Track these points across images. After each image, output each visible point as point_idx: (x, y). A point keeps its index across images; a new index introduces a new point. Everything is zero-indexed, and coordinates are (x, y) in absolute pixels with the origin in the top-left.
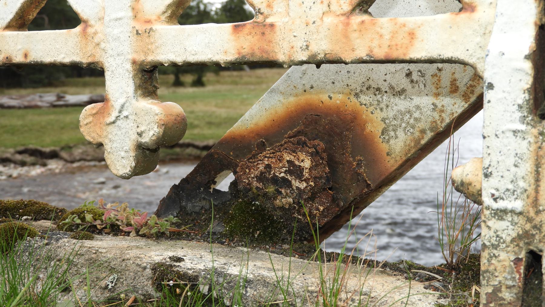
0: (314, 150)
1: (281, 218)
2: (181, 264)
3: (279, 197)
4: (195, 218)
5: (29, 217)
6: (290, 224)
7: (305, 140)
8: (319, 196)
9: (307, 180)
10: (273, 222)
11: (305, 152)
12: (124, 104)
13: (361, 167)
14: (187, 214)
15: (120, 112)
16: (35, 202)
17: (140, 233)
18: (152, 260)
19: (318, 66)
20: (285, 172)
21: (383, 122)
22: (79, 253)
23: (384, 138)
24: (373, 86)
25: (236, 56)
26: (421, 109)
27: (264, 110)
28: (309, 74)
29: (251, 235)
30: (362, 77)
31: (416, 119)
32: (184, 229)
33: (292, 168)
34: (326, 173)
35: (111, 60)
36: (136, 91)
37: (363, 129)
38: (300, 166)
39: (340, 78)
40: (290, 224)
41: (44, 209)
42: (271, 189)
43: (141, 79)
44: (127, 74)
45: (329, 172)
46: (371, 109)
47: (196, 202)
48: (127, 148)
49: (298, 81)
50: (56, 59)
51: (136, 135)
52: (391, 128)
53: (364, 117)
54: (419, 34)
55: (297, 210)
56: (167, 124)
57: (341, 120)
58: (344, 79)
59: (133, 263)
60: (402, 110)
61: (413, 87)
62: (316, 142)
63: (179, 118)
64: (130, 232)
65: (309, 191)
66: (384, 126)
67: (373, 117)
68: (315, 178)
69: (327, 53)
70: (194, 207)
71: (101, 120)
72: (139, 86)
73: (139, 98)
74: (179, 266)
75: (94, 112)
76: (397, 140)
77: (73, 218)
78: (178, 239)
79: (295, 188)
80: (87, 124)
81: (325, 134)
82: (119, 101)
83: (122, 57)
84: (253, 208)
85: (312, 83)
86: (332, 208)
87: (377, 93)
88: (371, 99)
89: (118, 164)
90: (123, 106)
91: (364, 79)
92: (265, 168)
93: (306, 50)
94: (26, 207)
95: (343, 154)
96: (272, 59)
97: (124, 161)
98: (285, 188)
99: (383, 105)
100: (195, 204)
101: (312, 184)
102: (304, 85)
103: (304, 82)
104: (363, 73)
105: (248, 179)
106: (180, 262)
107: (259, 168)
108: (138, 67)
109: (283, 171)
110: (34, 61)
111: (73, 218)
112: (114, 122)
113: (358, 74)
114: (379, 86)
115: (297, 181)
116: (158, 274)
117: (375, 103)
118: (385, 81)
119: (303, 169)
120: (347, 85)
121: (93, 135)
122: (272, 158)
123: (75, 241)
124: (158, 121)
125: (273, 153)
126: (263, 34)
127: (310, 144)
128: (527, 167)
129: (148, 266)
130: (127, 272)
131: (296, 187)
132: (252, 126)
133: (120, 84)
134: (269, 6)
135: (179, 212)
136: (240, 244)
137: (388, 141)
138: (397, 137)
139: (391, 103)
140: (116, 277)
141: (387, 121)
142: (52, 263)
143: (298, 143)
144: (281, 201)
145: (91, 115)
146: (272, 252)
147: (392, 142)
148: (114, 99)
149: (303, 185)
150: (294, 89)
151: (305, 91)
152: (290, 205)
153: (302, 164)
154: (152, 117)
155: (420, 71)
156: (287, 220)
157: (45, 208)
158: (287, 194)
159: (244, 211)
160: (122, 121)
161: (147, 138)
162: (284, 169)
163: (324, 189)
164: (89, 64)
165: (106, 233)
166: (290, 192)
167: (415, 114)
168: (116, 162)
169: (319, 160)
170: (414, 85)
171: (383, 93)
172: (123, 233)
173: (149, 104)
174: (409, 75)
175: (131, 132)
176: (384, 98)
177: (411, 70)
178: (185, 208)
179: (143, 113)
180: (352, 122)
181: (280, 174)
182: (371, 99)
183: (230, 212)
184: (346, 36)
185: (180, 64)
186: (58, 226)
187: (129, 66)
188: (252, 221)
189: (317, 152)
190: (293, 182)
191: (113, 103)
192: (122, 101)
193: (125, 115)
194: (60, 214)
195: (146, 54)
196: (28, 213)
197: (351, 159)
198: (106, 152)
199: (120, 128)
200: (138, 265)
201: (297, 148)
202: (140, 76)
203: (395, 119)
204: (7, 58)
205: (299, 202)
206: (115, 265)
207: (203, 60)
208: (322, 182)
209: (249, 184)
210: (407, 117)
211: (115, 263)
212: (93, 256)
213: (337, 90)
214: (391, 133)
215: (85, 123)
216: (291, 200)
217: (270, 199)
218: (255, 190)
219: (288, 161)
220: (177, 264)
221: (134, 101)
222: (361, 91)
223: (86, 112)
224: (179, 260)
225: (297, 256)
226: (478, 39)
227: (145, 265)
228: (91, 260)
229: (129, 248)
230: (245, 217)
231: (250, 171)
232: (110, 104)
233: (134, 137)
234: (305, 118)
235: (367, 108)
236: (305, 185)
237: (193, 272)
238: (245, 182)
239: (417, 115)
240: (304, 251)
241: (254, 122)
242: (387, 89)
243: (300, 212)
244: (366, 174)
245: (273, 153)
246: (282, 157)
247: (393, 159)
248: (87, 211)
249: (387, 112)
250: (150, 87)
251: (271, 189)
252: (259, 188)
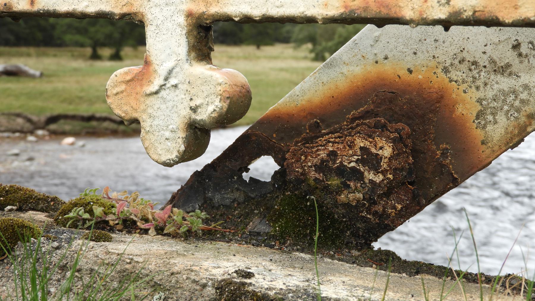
0: (396, 135)
1: (344, 217)
2: (252, 281)
3: (345, 192)
4: (224, 213)
5: (15, 208)
6: (354, 224)
7: (385, 122)
8: (396, 192)
9: (384, 172)
10: (334, 221)
11: (385, 137)
12: (173, 69)
13: (447, 157)
14: (213, 207)
15: (166, 79)
16: (18, 188)
17: (165, 232)
18: (211, 275)
19: (447, 29)
20: (357, 161)
21: (478, 104)
22: (106, 262)
23: (479, 123)
24: (468, 59)
25: (342, 10)
26: (530, 89)
27: (321, 84)
28: (383, 42)
29: (308, 238)
30: (454, 47)
31: (522, 101)
32: (214, 227)
33: (365, 156)
34: (409, 164)
35: (156, 11)
36: (189, 52)
37: (453, 111)
38: (377, 154)
39: (424, 48)
40: (354, 224)
41: (31, 197)
42: (335, 182)
43: (196, 37)
44: (179, 30)
45: (413, 163)
46: (464, 87)
47: (227, 194)
48: (174, 127)
49: (368, 50)
50: (76, 7)
51: (188, 110)
52: (489, 111)
53: (454, 96)
55: (367, 208)
56: (232, 97)
57: (424, 99)
58: (429, 49)
59: (187, 278)
60: (505, 89)
61: (521, 62)
62: (400, 125)
63: (244, 90)
64: (149, 229)
65: (385, 185)
66: (480, 108)
67: (467, 96)
68: (396, 169)
69: (477, 9)
70: (223, 198)
71: (138, 89)
72: (193, 46)
73: (193, 62)
74: (251, 283)
75: (128, 78)
76: (496, 126)
77: (79, 211)
78: (212, 240)
79: (367, 181)
80: (117, 94)
81: (403, 116)
82: (164, 64)
83: (173, 8)
84: (308, 204)
85: (387, 52)
86: (412, 207)
87: (473, 67)
88: (464, 75)
89: (160, 147)
90: (170, 72)
91: (456, 50)
92: (328, 155)
93: (447, 6)
94: (7, 195)
95: (424, 141)
96: (395, 15)
97: (169, 144)
98: (355, 180)
99: (479, 83)
100: (225, 196)
101: (391, 176)
102: (376, 54)
103: (375, 52)
104: (456, 42)
105: (302, 167)
106: (249, 278)
107: (319, 155)
108: (194, 21)
109: (353, 159)
110: (44, 10)
111: (79, 211)
112: (156, 93)
113: (449, 43)
114: (476, 59)
115: (372, 172)
116: (227, 296)
117: (469, 80)
118: (484, 53)
119: (381, 158)
120: (434, 56)
121: (125, 108)
122: (338, 143)
123: (92, 243)
124: (221, 92)
125: (339, 137)
127: (392, 128)
129: (210, 283)
130: (179, 291)
131: (370, 180)
132: (304, 102)
133: (167, 41)
135: (202, 205)
136: (295, 248)
137: (484, 127)
138: (496, 122)
139: (491, 80)
140: (163, 297)
141: (484, 103)
142: (69, 274)
143: (376, 126)
144: (347, 197)
145: (123, 82)
146: (339, 260)
147: (489, 128)
148: (157, 62)
149: (379, 178)
150: (362, 59)
151: (377, 62)
152: (358, 201)
153: (380, 152)
154: (212, 87)
155: (531, 43)
156: (350, 220)
157: (32, 196)
158: (356, 188)
159: (297, 207)
160: (167, 91)
162: (356, 157)
163: (403, 184)
164: (123, 16)
165: (119, 230)
166: (361, 186)
167: (521, 95)
168: (156, 145)
169: (402, 147)
170: (522, 59)
171: (481, 68)
172: (139, 231)
173: (208, 70)
174: (516, 46)
175: (181, 106)
176: (482, 74)
177: (520, 41)
178: (211, 200)
179: (199, 82)
180: (438, 102)
181: (350, 163)
182: (464, 75)
183: (276, 207)
185: (258, 18)
186: (56, 220)
187: (182, 20)
188: (308, 220)
189: (401, 138)
190: (366, 173)
191: (157, 68)
192: (169, 65)
193: (174, 84)
194: (52, 203)
195: (207, 4)
196: (11, 202)
197: (434, 147)
198: (142, 130)
199: (164, 100)
200: (194, 281)
201: (375, 132)
202: (195, 33)
203: (495, 100)
204: (5, 5)
205: (370, 198)
206: (161, 280)
207: (293, 14)
208: (402, 175)
209: (304, 174)
210: (511, 98)
211: (160, 277)
212: (127, 266)
213: (419, 62)
214: (488, 117)
215: (115, 92)
216: (361, 196)
217: (331, 193)
218: (312, 182)
219: (361, 148)
220: (248, 281)
221: (186, 66)
222: (452, 65)
223: (116, 78)
224: (249, 275)
225: (374, 266)
227: (204, 281)
228: (125, 271)
229: (170, 255)
230: (299, 215)
231: (306, 159)
232: (151, 68)
233: (185, 112)
234: (376, 96)
235: (458, 85)
236: (381, 177)
237: (276, 293)
238: (298, 171)
239: (524, 96)
240: (382, 260)
241: (306, 97)
242: (486, 64)
243: (370, 210)
244: (453, 166)
245: (339, 137)
246: (353, 142)
247: (490, 149)
248: (94, 202)
249: (485, 91)
250: (204, 48)
251: (335, 182)
252: (319, 179)
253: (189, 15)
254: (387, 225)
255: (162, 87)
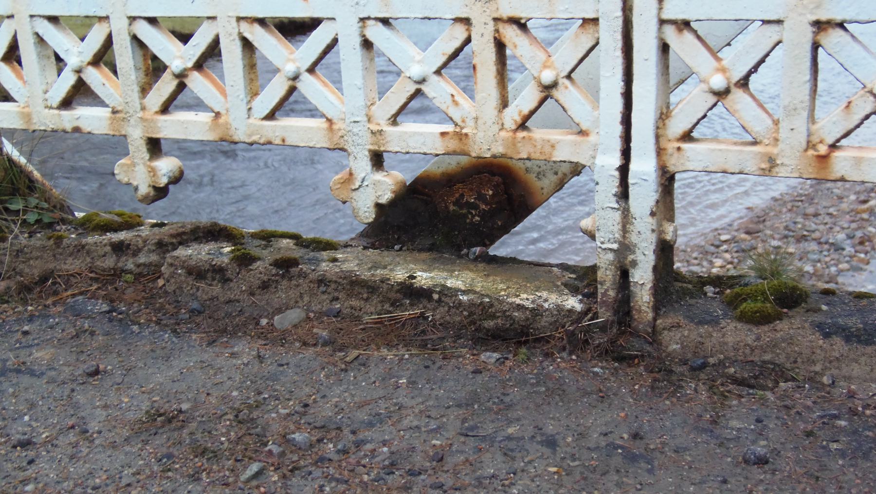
54: (557, 146)
126: (461, 139)
128: (617, 228)
134: (463, 121)
161: (384, 200)
184: (514, 145)
187: (367, 153)
192: (363, 175)
226: (591, 153)
253: (370, 151)
254: (492, 237)
255: (360, 186)
